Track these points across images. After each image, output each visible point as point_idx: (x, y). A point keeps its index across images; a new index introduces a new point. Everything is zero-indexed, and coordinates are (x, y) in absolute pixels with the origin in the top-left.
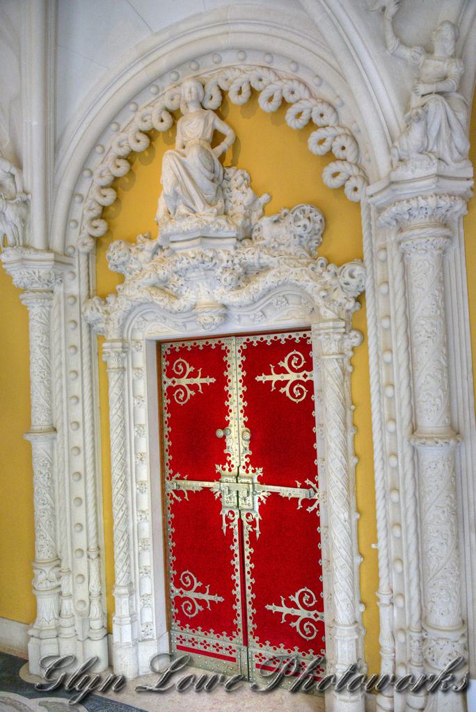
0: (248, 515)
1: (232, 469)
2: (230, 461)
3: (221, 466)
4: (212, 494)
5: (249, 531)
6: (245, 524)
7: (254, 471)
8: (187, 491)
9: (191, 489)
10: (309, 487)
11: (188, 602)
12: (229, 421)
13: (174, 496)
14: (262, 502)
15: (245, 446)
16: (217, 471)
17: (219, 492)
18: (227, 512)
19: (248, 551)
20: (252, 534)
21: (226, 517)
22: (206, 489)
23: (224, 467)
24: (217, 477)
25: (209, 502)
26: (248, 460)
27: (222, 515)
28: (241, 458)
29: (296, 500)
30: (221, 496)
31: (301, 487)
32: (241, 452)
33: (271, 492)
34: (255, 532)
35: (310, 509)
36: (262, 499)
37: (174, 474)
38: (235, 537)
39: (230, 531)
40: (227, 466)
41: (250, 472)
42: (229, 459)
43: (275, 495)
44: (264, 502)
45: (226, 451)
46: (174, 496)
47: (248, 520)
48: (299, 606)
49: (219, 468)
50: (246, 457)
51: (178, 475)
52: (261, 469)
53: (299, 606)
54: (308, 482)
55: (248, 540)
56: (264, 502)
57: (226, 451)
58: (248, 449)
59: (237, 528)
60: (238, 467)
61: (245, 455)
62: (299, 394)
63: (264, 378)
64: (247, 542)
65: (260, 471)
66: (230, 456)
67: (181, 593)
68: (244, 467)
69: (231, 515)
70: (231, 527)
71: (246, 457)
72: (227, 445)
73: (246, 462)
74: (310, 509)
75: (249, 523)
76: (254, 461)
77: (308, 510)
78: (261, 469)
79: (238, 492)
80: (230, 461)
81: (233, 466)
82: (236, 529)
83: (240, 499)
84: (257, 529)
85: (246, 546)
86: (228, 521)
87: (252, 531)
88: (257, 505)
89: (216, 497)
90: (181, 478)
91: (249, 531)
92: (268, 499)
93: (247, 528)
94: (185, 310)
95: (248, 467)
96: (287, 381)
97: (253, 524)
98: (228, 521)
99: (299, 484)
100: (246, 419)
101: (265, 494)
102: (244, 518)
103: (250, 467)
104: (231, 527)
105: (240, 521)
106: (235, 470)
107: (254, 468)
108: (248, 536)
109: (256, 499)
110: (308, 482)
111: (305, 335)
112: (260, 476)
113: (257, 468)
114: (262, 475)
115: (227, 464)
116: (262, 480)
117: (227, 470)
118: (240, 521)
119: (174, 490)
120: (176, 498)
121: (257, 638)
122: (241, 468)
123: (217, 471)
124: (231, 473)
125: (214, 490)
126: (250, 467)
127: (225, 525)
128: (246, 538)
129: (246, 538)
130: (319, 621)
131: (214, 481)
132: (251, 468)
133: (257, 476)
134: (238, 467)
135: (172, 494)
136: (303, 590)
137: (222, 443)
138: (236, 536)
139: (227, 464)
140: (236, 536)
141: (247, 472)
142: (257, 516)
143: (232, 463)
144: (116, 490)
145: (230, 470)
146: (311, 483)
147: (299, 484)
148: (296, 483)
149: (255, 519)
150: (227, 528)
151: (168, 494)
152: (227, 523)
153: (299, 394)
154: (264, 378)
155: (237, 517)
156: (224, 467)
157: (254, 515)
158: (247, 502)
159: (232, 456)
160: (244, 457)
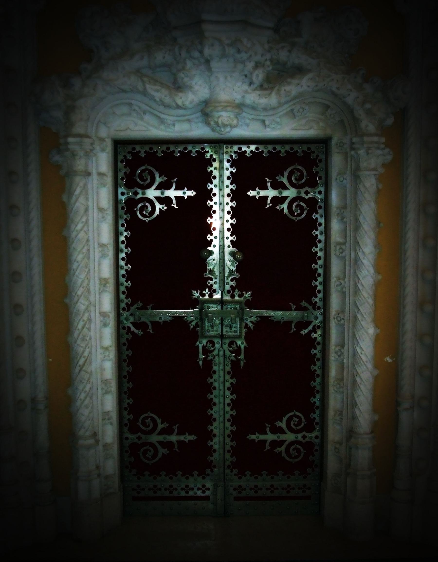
8: (152, 322)
9: (157, 319)
10: (305, 309)
11: (148, 447)
12: (212, 240)
13: (133, 329)
17: (196, 321)
18: (204, 342)
23: (204, 292)
25: (183, 335)
27: (198, 346)
28: (226, 281)
29: (288, 323)
31: (296, 310)
32: (226, 275)
33: (260, 317)
35: (304, 332)
36: (250, 324)
37: (132, 304)
39: (208, 364)
43: (264, 320)
44: (252, 327)
46: (133, 329)
48: (287, 431)
51: (140, 304)
53: (287, 431)
54: (304, 304)
56: (252, 327)
61: (231, 278)
62: (299, 212)
63: (258, 193)
65: (247, 295)
66: (211, 279)
67: (139, 438)
69: (209, 345)
71: (232, 280)
74: (304, 332)
75: (232, 352)
77: (302, 332)
80: (212, 286)
81: (215, 291)
84: (242, 357)
86: (206, 351)
89: (192, 327)
90: (144, 308)
94: (190, 106)
96: (287, 197)
99: (293, 307)
100: (234, 238)
101: (254, 319)
107: (242, 291)
108: (230, 366)
109: (244, 324)
110: (304, 304)
111: (309, 149)
112: (248, 300)
116: (249, 304)
117: (207, 295)
119: (131, 323)
120: (136, 331)
121: (235, 471)
126: (236, 290)
127: (202, 356)
130: (307, 442)
132: (237, 292)
135: (129, 327)
136: (292, 414)
141: (233, 296)
144: (81, 323)
145: (211, 296)
146: (307, 305)
147: (293, 307)
148: (291, 306)
151: (124, 328)
153: (299, 212)
154: (258, 193)
156: (204, 292)
157: (239, 343)
158: (233, 329)
159: (214, 280)
160: (229, 281)
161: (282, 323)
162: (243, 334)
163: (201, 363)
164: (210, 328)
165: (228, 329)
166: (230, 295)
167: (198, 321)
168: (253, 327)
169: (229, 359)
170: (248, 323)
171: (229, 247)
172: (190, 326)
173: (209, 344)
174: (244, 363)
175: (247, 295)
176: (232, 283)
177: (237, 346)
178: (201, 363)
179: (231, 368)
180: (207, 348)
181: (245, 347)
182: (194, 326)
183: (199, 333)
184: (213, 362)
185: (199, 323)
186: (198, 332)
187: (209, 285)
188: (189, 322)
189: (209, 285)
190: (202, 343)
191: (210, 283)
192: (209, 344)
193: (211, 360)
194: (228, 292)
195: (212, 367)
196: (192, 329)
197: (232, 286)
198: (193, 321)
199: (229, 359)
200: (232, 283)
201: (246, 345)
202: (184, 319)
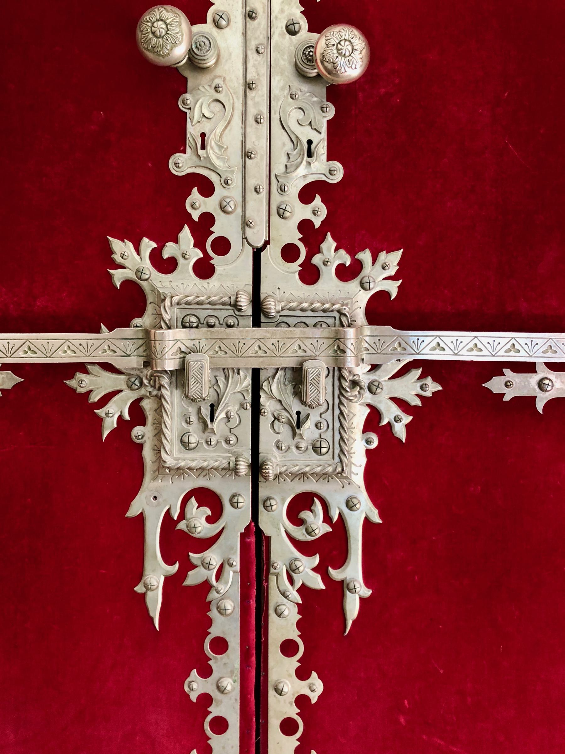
0: (301, 504)
1: (216, 260)
2: (208, 219)
3: (148, 245)
4: (85, 409)
5: (304, 590)
6: (282, 552)
7: (346, 273)
14: (386, 433)
15: (305, 134)
16: (118, 277)
19: (289, 686)
20: (318, 607)
21: (169, 523)
22: (46, 379)
23: (170, 250)
24: (128, 304)
26: (317, 211)
27: (141, 518)
28: (276, 198)
30: (137, 414)
34: (337, 590)
36: (390, 413)
38: (215, 631)
40: (185, 247)
41: (328, 274)
42: (197, 204)
45: (182, 164)
47: (299, 533)
49: (130, 259)
50: (307, 194)
52: (392, 259)
55: (294, 634)
57: (182, 164)
58: (322, 150)
59: (232, 576)
60: (257, 253)
64: (288, 648)
65: (382, 272)
66: (207, 188)
68: (289, 252)
70: (193, 578)
71: (307, 194)
72: (193, 131)
73: (305, 226)
75: (305, 548)
76: (351, 215)
78: (392, 259)
79: (256, 373)
80: (208, 219)
81: (222, 246)
82: (227, 595)
83: (264, 423)
84: (353, 571)
85: (282, 670)
87: (317, 583)
88: (359, 448)
89: (110, 424)
91: (304, 590)
92: (422, 414)
93: (294, 572)
95: (314, 248)
97: (331, 549)
98: (179, 544)
101: (411, 388)
102: (276, 524)
103: (329, 244)
104: (193, 578)
105: (256, 546)
106: (232, 275)
107: (352, 253)
109: (358, 415)
112: (383, 295)
113: (365, 256)
114: (393, 288)
115: (186, 234)
117: (186, 267)
118: (256, 546)
122: (272, 259)
123: (118, 277)
124: (213, 287)
125: (94, 384)
126: (329, 244)
128: (284, 623)
129: (284, 623)
131: (98, 331)
132: (331, 254)
133: (364, 297)
134: (257, 253)
137: (162, 93)
138: (226, 622)
139: (186, 234)
140: (226, 622)
141: (310, 275)
142: (350, 505)
143: (218, 230)
145: (204, 270)
149: (340, 528)
150: (172, 584)
152: (168, 560)
155: (236, 519)
156: (170, 250)
159: (219, 192)
161: (540, 406)
162: (358, 461)
163: (155, 603)
164: (195, 427)
165: (284, 431)
166: (296, 267)
167: (143, 392)
168: (408, 427)
169: (291, 581)
170: (382, 407)
171: (291, 30)
172: (100, 421)
173: (193, 501)
174: (362, 600)
175: (382, 272)
176: (303, 212)
177: (327, 519)
178: (155, 603)
179: (299, 625)
180: (182, 526)
181: (367, 521)
182: (120, 418)
183: (147, 454)
184: (213, 596)
185: (147, 405)
186: (141, 447)
187: (196, 216)
188: (95, 398)
189: (196, 216)
190: (153, 502)
191: (197, 204)
192: (193, 501)
193: (206, 586)
194: (289, 252)
195: (209, 622)
196: (113, 433)
197: (305, 226)
198: (120, 391)
199: (291, 581)
200: (303, 212)
201: (376, 518)
202: (72, 383)
